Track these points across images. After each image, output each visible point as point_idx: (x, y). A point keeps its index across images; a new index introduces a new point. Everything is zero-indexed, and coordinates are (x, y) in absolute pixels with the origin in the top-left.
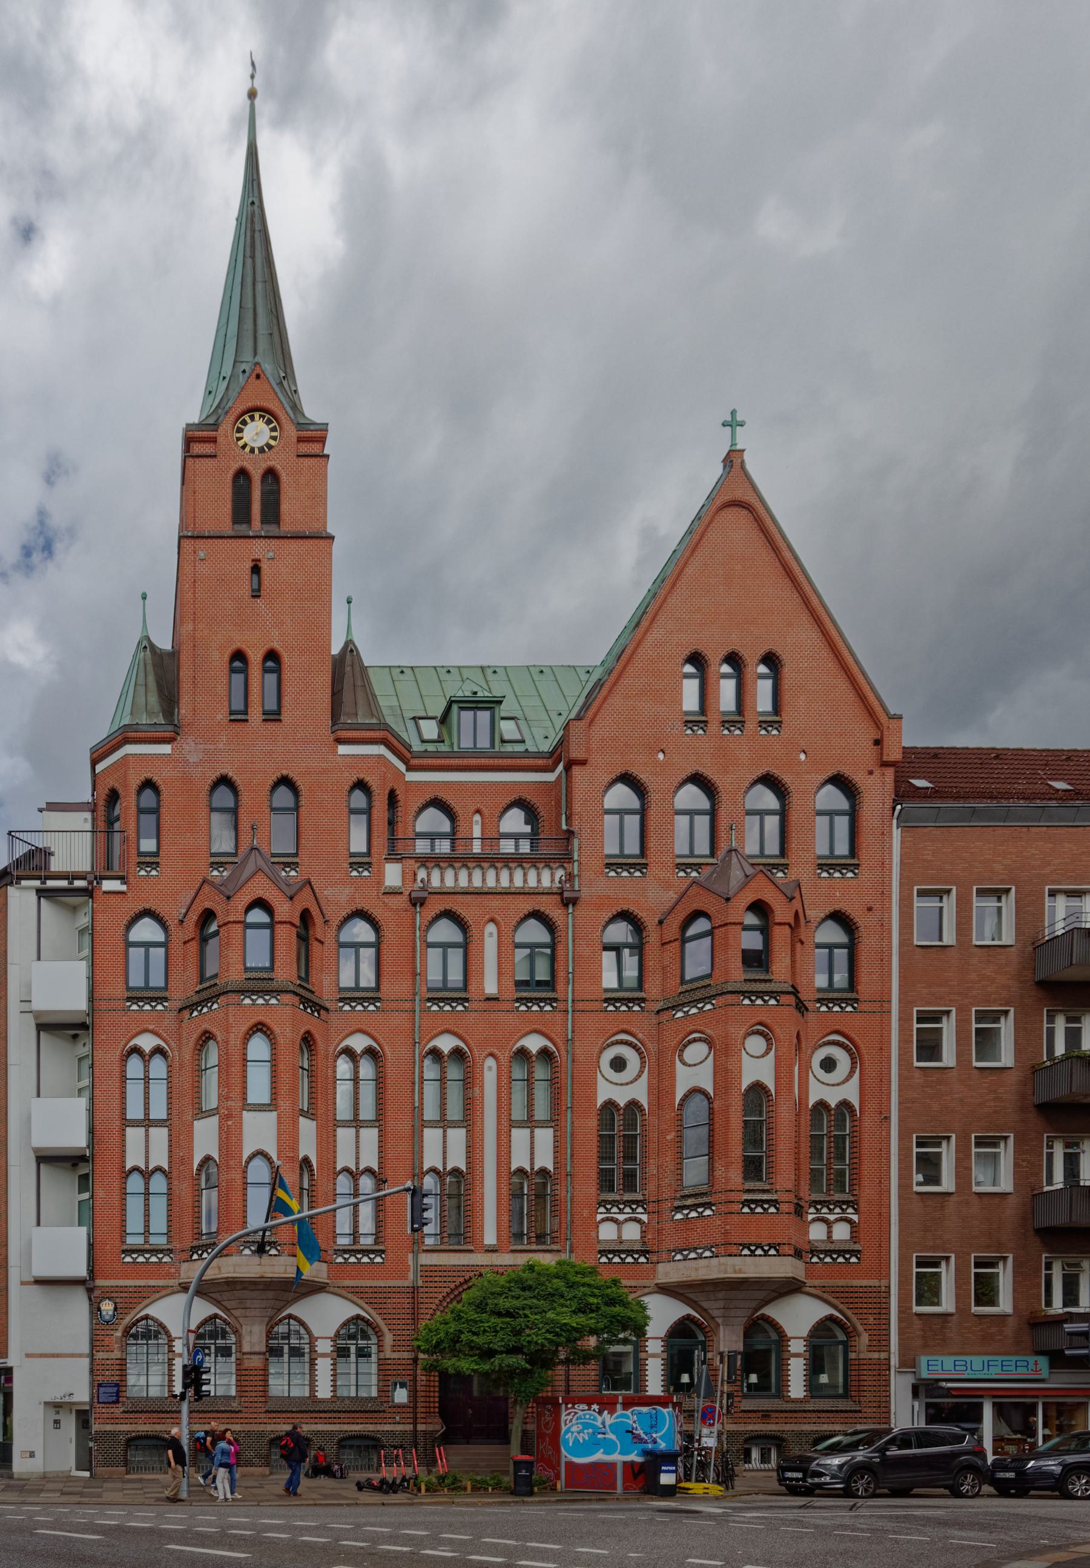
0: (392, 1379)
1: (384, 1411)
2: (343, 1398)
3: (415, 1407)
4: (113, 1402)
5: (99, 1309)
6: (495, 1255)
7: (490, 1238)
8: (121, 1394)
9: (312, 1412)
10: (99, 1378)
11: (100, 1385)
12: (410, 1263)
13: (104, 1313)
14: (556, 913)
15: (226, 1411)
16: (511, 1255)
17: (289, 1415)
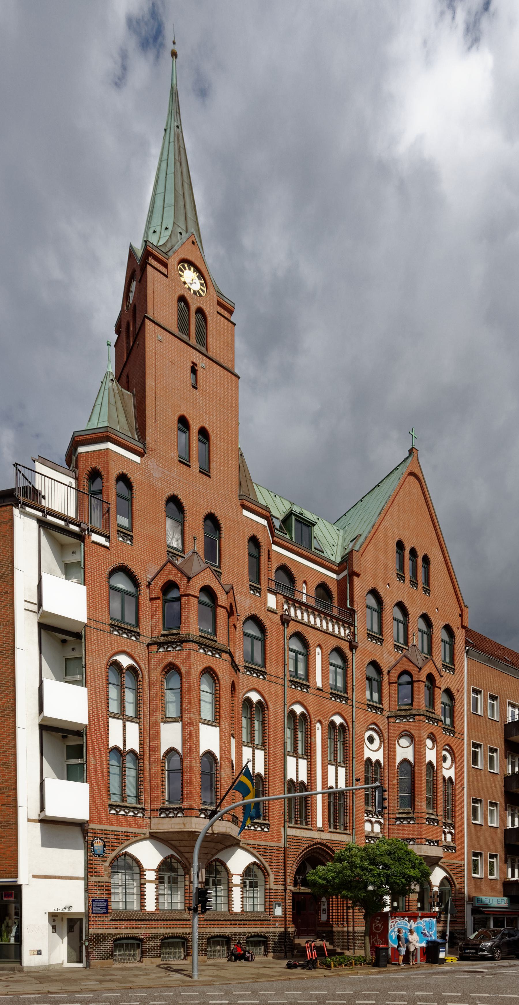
0: (274, 901)
1: (270, 920)
2: (247, 912)
3: (286, 918)
4: (104, 913)
5: (92, 845)
6: (322, 833)
7: (319, 824)
8: (109, 907)
9: (231, 920)
10: (92, 895)
11: (93, 901)
12: (283, 833)
13: (96, 848)
14: (347, 651)
15: (181, 920)
16: (329, 834)
17: (218, 922)
